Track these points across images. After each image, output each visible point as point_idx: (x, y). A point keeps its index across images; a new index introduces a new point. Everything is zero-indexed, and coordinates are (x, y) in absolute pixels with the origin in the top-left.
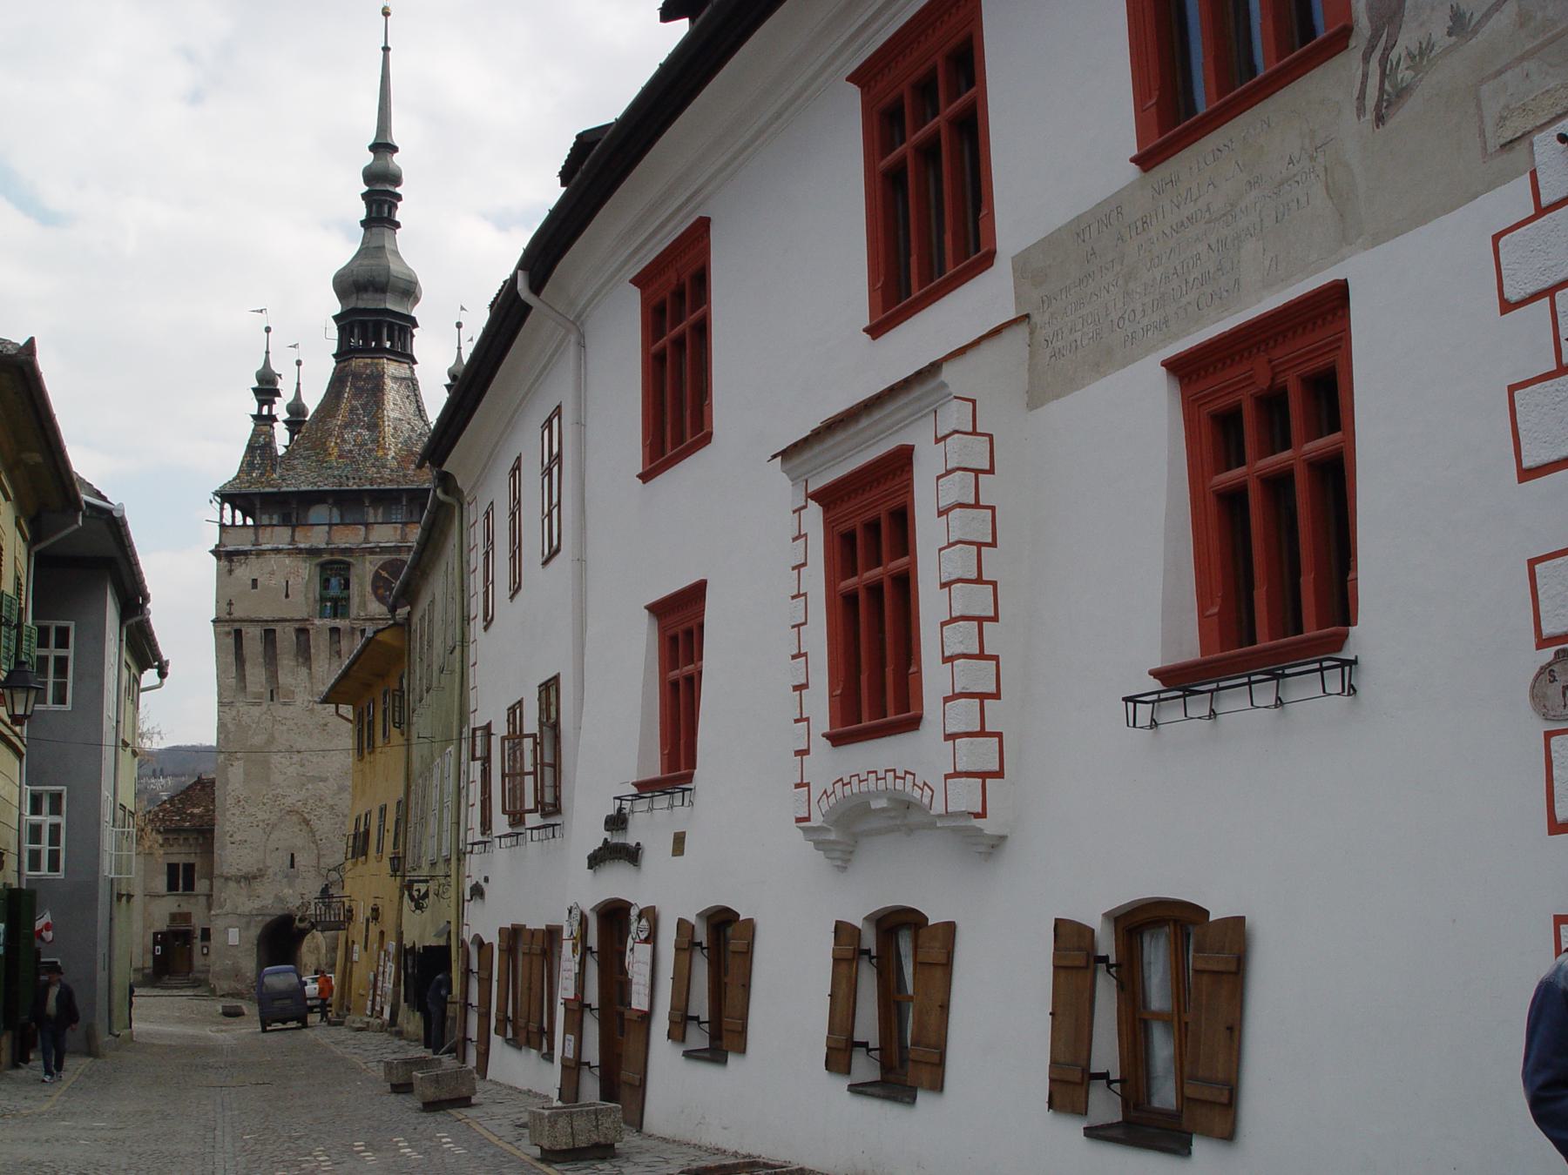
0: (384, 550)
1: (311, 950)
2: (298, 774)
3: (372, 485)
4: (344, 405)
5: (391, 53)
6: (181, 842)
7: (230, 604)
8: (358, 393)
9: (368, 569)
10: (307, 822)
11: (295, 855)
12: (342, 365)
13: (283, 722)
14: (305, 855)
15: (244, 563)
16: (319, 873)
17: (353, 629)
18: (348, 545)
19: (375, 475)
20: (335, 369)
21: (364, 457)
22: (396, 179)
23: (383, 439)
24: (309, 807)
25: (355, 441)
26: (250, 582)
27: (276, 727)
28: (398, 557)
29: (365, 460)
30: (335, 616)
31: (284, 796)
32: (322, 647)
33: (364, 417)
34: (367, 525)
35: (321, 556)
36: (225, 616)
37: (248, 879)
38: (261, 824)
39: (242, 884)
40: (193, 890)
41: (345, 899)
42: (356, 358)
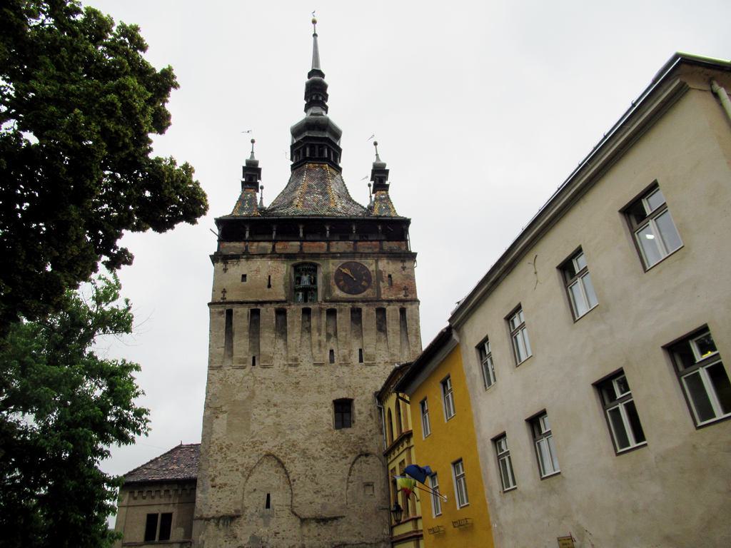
0: (343, 255)
2: (274, 423)
5: (318, 38)
6: (162, 494)
7: (224, 291)
10: (282, 464)
13: (263, 381)
14: (280, 495)
16: (293, 512)
24: (284, 451)
26: (240, 277)
27: (256, 385)
31: (262, 443)
32: (296, 323)
36: (219, 299)
37: (229, 519)
38: (240, 468)
39: (221, 525)
40: (169, 538)
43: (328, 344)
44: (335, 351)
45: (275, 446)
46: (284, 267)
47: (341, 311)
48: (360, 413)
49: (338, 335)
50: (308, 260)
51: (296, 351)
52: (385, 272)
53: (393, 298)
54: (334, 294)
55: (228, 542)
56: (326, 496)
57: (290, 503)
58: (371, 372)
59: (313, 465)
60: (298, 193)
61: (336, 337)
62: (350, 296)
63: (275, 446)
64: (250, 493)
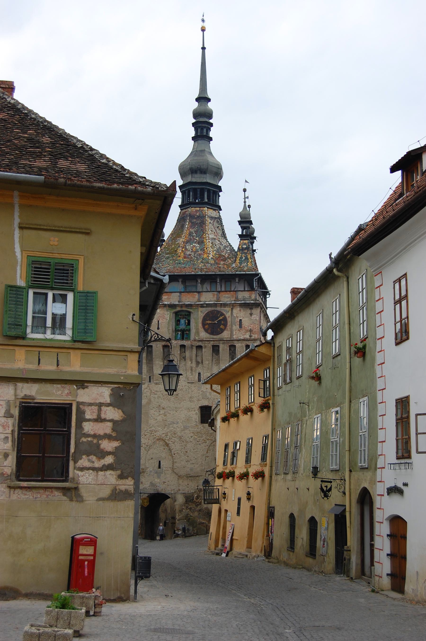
0: (208, 305)
1: (163, 511)
2: (163, 420)
3: (201, 272)
4: (186, 232)
8: (193, 225)
9: (200, 315)
10: (167, 445)
11: (161, 462)
12: (184, 211)
13: (156, 393)
16: (173, 472)
17: (192, 346)
18: (189, 303)
19: (203, 267)
20: (180, 213)
21: (197, 258)
22: (210, 115)
23: (207, 249)
24: (168, 437)
25: (192, 250)
27: (152, 395)
28: (215, 309)
29: (198, 259)
30: (183, 339)
31: (156, 431)
33: (196, 238)
34: (199, 292)
35: (176, 309)
41: (218, 487)
42: (192, 207)
43: (197, 368)
44: (201, 374)
45: (164, 434)
46: (168, 315)
47: (205, 347)
49: (204, 363)
50: (184, 309)
52: (237, 317)
53: (242, 338)
54: (201, 335)
57: (172, 467)
60: (181, 241)
61: (203, 364)
62: (212, 336)
63: (164, 434)
64: (149, 460)
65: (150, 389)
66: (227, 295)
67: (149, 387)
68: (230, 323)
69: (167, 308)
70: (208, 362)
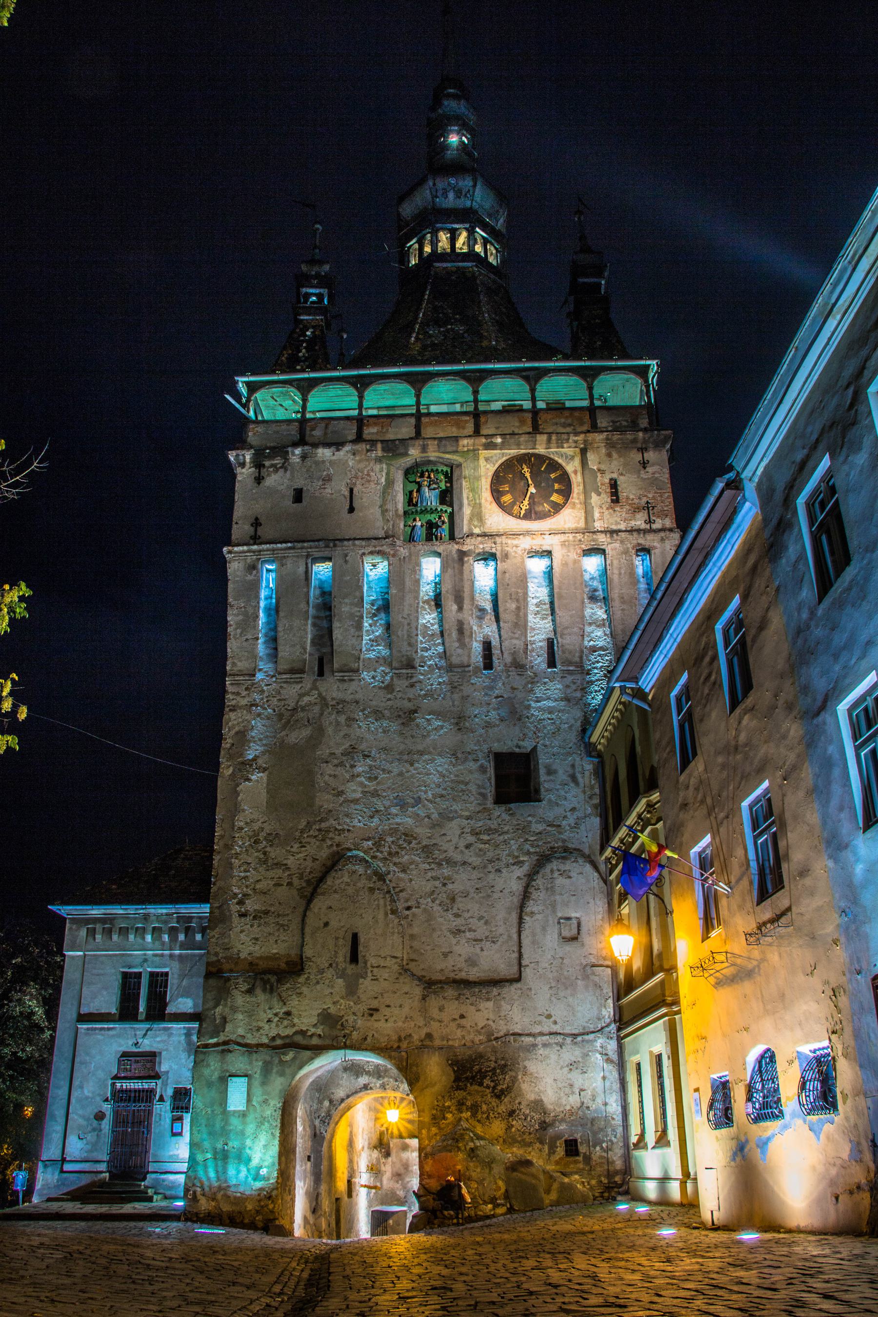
9: (482, 471)
15: (281, 467)
28: (531, 451)
35: (406, 454)
38: (296, 882)
44: (493, 643)
46: (381, 470)
48: (550, 772)
51: (410, 644)
53: (622, 526)
55: (273, 1025)
56: (475, 940)
58: (574, 687)
59: (449, 878)
63: (368, 839)
65: (320, 695)
66: (563, 420)
67: (316, 688)
68: (581, 487)
69: (380, 453)
70: (514, 606)
